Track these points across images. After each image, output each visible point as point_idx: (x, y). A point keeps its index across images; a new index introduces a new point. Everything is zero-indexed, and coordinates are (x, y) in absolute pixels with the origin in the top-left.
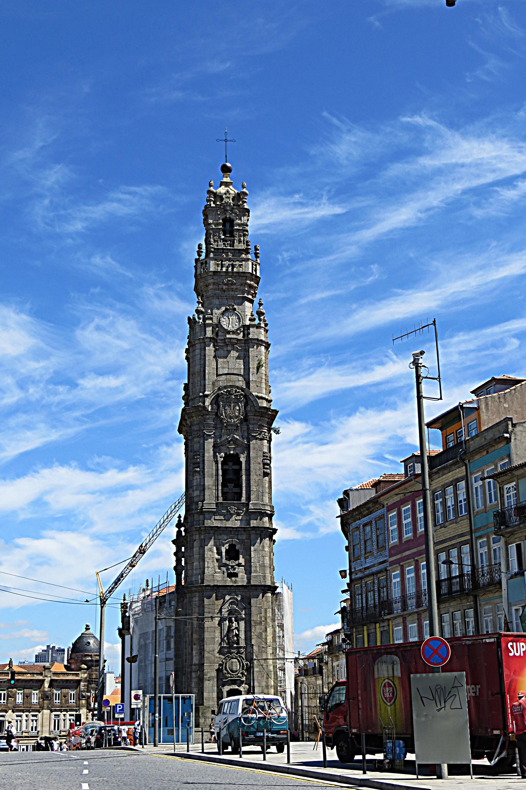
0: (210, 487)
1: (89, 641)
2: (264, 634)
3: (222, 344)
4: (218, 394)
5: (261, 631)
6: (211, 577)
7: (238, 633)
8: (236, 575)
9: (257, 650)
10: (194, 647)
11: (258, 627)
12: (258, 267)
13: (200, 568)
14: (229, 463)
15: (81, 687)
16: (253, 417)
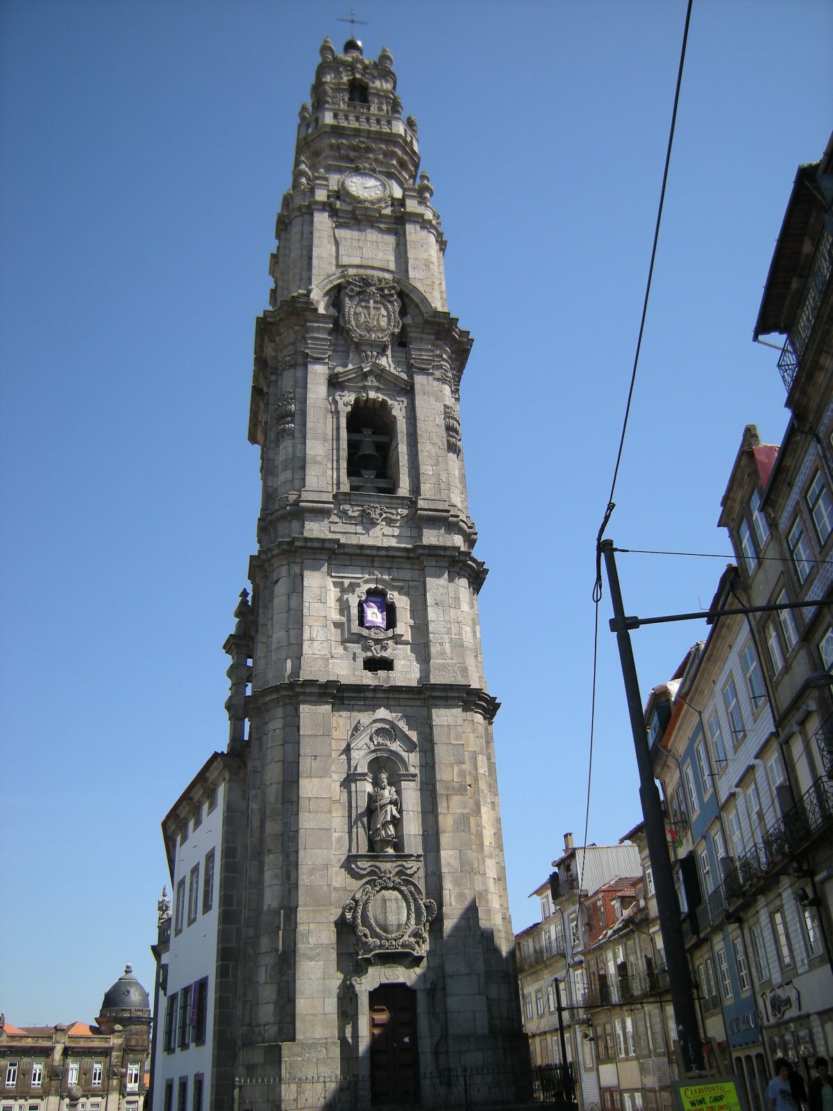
0: (319, 458)
1: (129, 988)
2: (472, 820)
3: (347, 221)
4: (339, 285)
5: (465, 811)
6: (321, 663)
7: (398, 816)
8: (387, 665)
9: (456, 864)
10: (269, 859)
11: (455, 799)
12: (415, 142)
13: (289, 644)
14: (363, 429)
15: (113, 1059)
16: (419, 335)
